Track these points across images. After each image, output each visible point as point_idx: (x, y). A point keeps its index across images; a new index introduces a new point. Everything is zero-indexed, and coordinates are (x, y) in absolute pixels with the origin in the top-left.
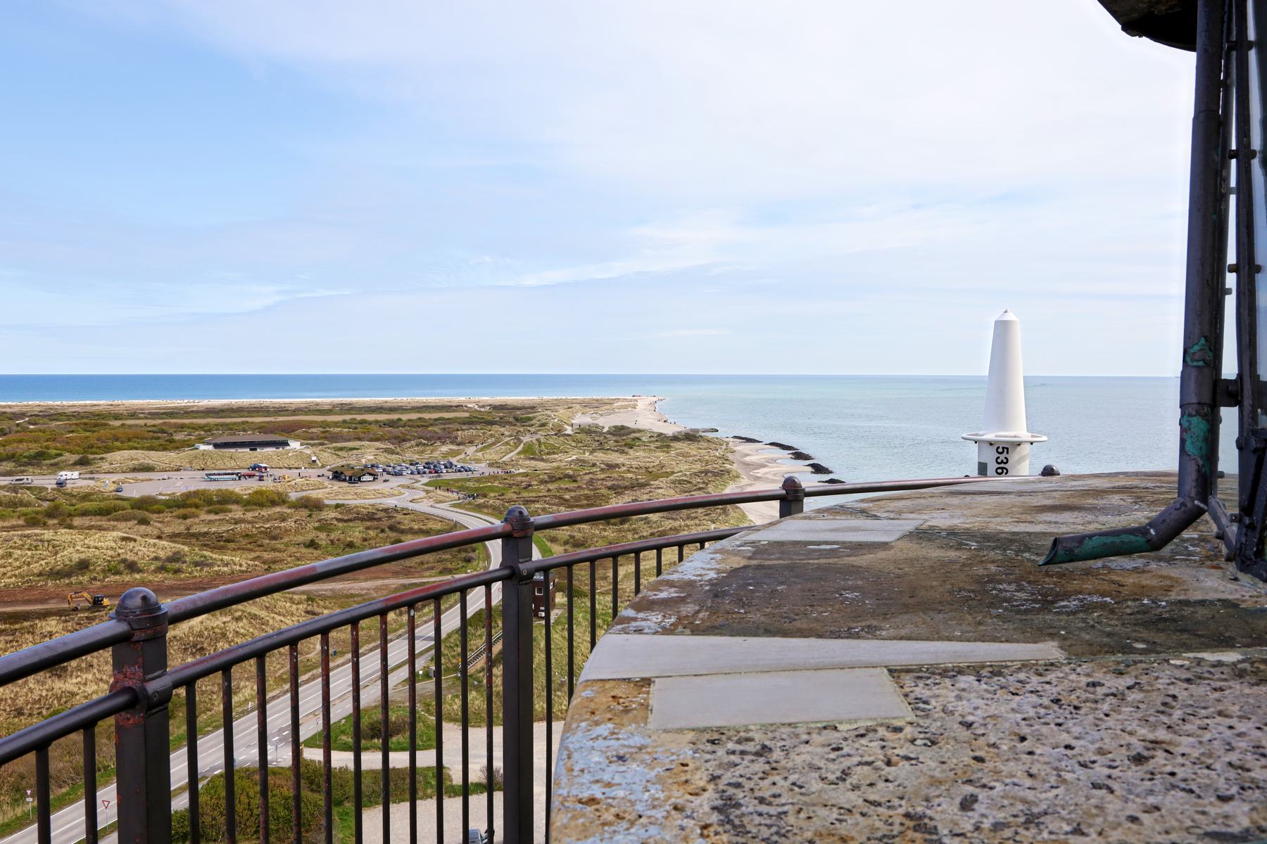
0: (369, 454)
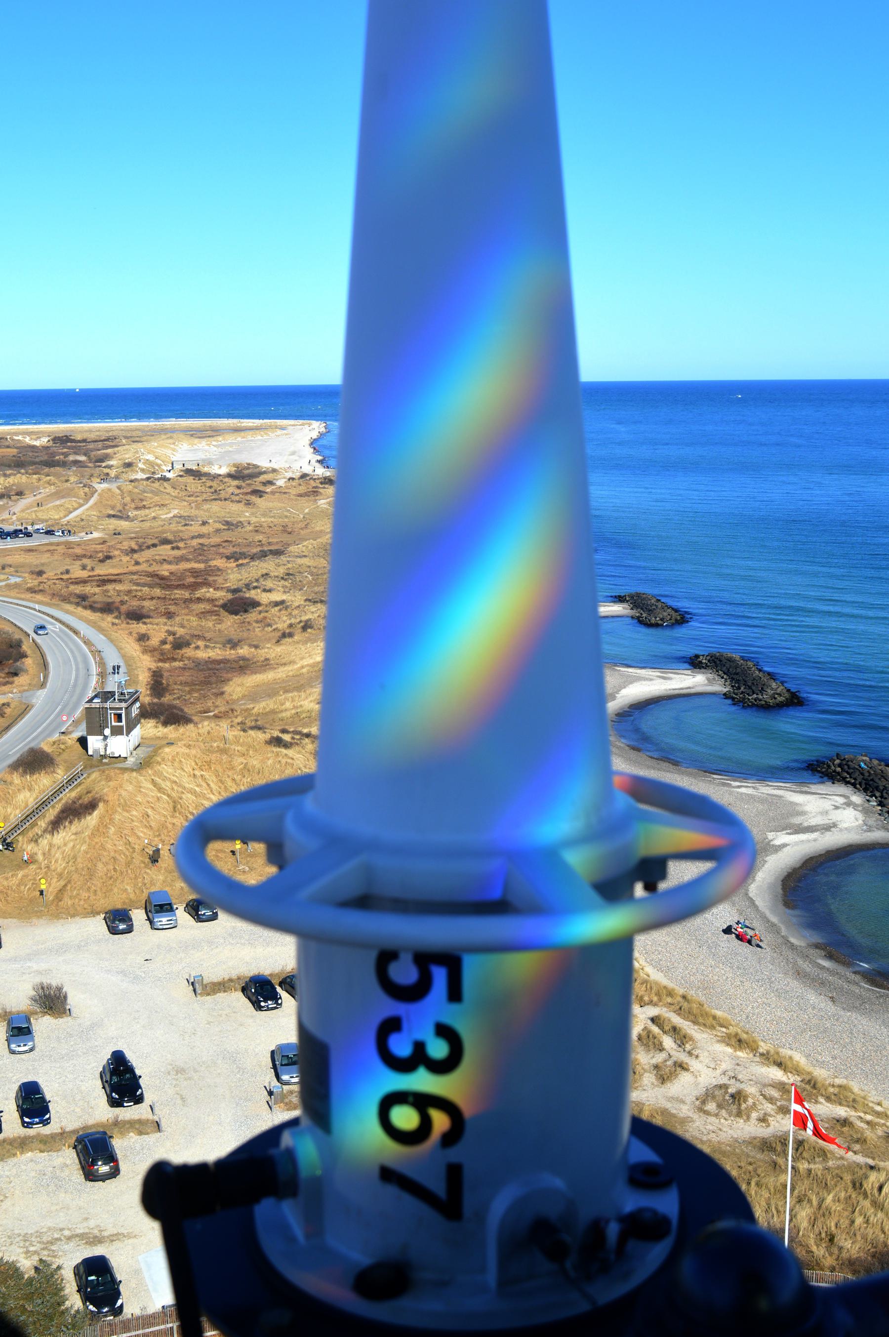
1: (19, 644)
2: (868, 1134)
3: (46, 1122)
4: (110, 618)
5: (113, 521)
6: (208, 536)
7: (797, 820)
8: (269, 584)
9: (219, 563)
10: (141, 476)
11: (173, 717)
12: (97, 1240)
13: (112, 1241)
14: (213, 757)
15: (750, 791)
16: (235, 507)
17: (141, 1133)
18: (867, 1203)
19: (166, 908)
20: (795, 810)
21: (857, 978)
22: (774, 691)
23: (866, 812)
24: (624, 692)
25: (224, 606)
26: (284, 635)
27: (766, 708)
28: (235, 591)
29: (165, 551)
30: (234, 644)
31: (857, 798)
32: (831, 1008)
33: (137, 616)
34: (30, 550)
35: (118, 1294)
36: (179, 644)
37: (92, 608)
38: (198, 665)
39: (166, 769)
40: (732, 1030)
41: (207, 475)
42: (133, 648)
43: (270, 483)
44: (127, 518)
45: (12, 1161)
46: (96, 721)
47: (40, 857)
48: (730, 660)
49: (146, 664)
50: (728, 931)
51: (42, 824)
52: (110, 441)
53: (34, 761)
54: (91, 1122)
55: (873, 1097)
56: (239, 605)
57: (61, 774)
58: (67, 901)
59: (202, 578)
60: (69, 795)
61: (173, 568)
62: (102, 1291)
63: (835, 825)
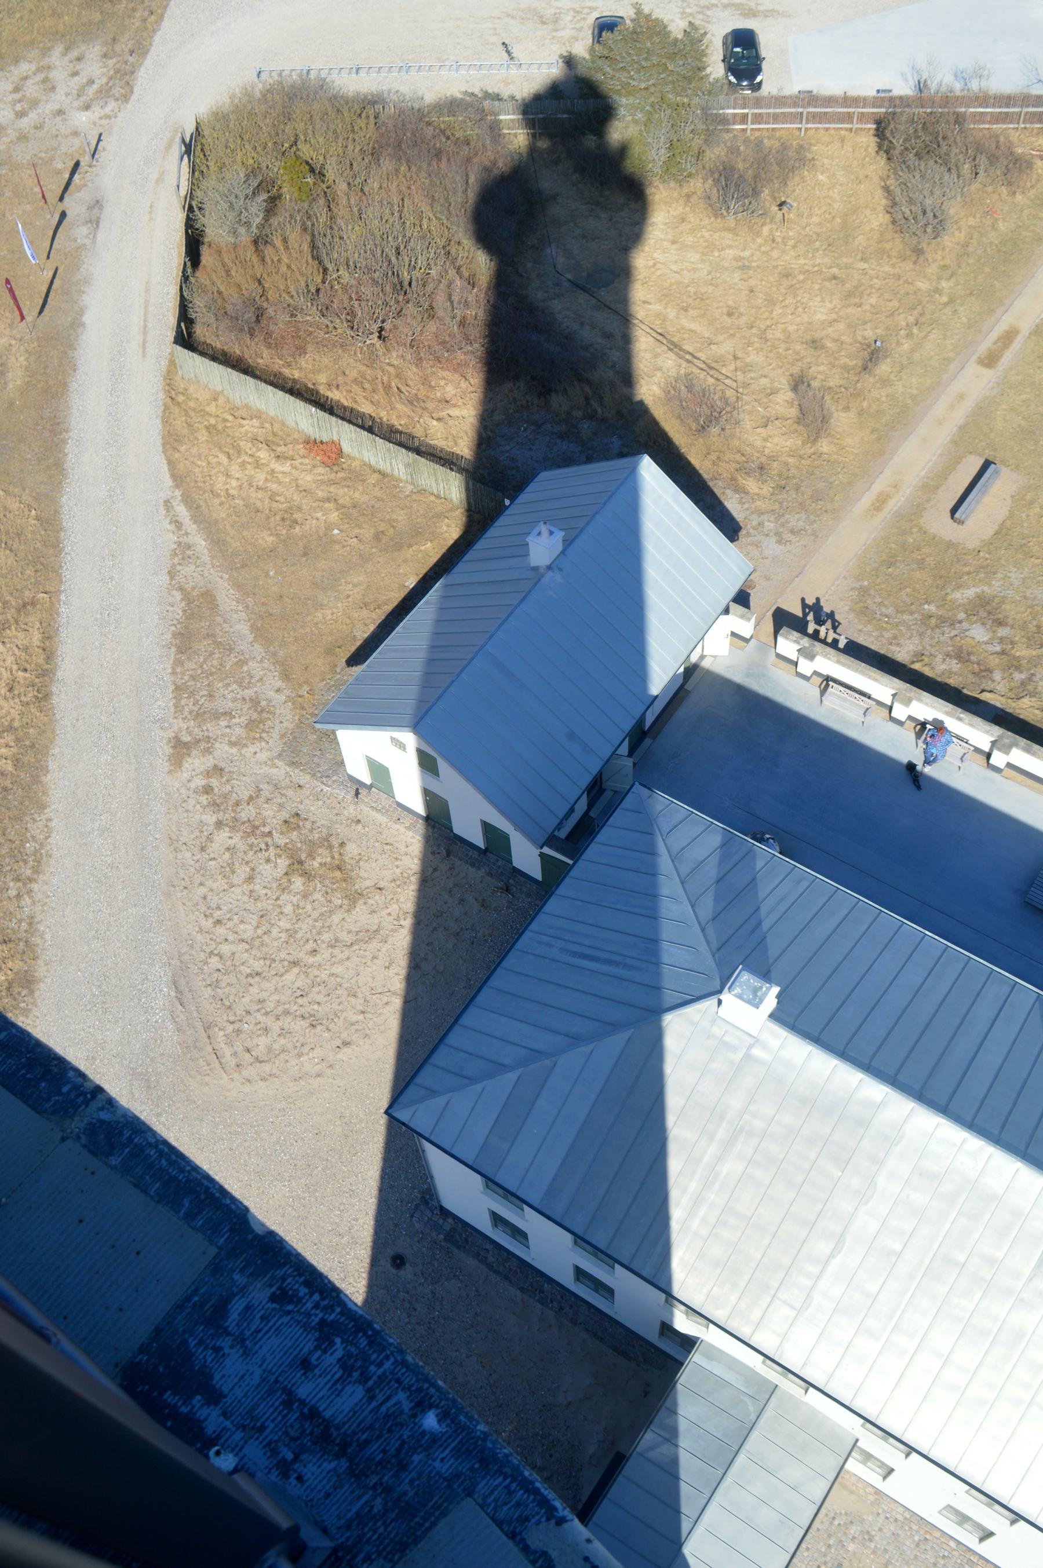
12: (752, 13)
13: (766, 16)
35: (758, 70)
62: (745, 64)
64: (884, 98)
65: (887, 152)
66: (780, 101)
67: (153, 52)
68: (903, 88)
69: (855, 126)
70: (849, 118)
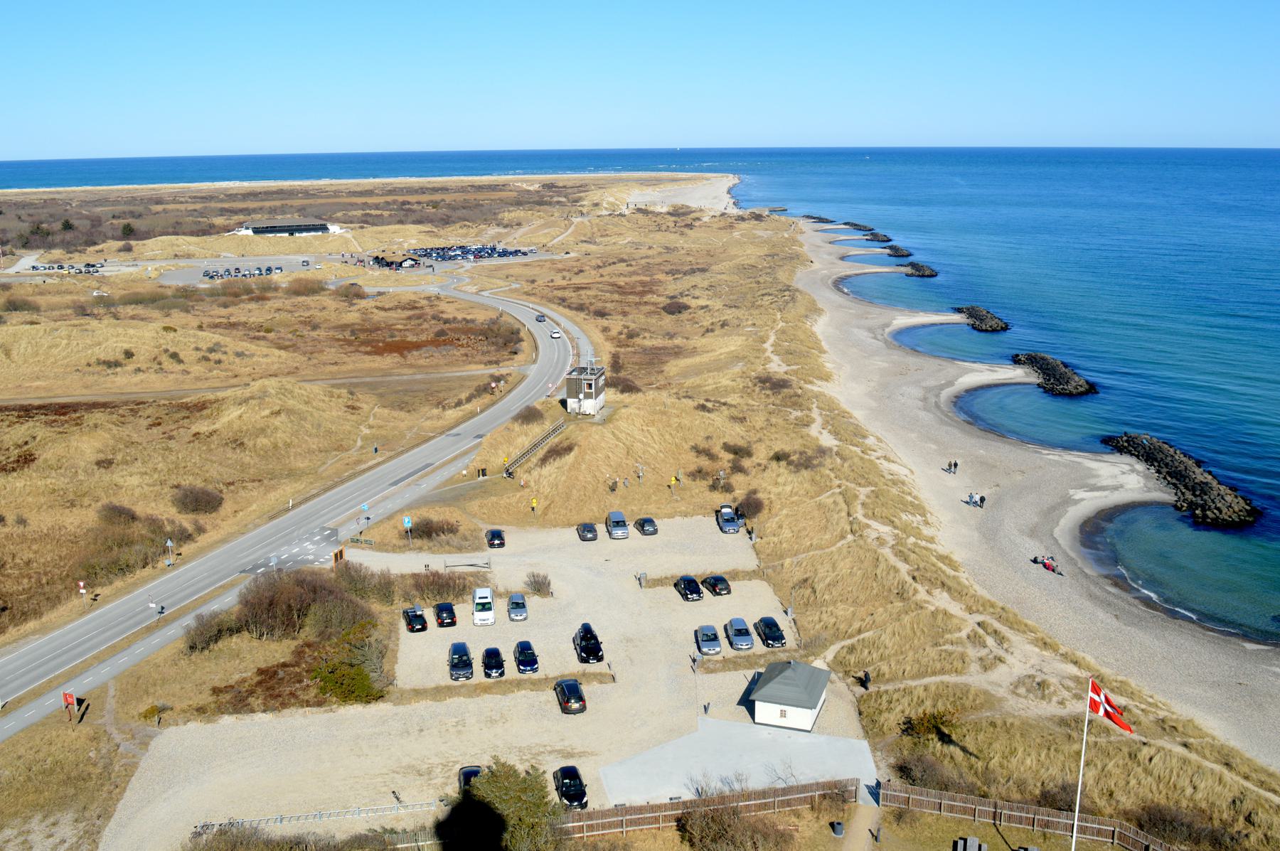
0: (411, 237)
1: (518, 332)
2: (1143, 718)
3: (535, 670)
4: (582, 315)
5: (585, 245)
6: (653, 257)
7: (1092, 481)
8: (697, 293)
9: (661, 277)
10: (605, 213)
11: (628, 387)
12: (570, 755)
14: (656, 417)
15: (1056, 458)
16: (673, 237)
17: (601, 682)
18: (1140, 770)
19: (620, 524)
20: (1091, 474)
21: (1136, 602)
22: (1077, 383)
23: (1146, 477)
24: (961, 380)
25: (664, 308)
26: (708, 331)
27: (1070, 396)
28: (672, 297)
29: (621, 267)
30: (671, 336)
31: (1140, 466)
32: (1115, 622)
33: (601, 314)
34: (526, 265)
35: (584, 794)
36: (631, 335)
37: (569, 307)
38: (645, 350)
39: (622, 424)
40: (1039, 635)
41: (652, 212)
42: (599, 337)
43: (698, 219)
44: (595, 243)
45: (511, 696)
46: (574, 388)
47: (532, 484)
48: (1043, 359)
49: (609, 348)
50: (1035, 561)
51: (534, 460)
52: (583, 187)
53: (529, 415)
54: (567, 672)
55: (1146, 691)
56: (675, 308)
57: (548, 425)
58: (551, 516)
59: (647, 288)
60: (554, 440)
61: (627, 279)
63: (1122, 486)
64: (674, 803)
65: (690, 841)
66: (604, 814)
67: (117, 816)
68: (688, 796)
69: (662, 825)
70: (656, 820)
